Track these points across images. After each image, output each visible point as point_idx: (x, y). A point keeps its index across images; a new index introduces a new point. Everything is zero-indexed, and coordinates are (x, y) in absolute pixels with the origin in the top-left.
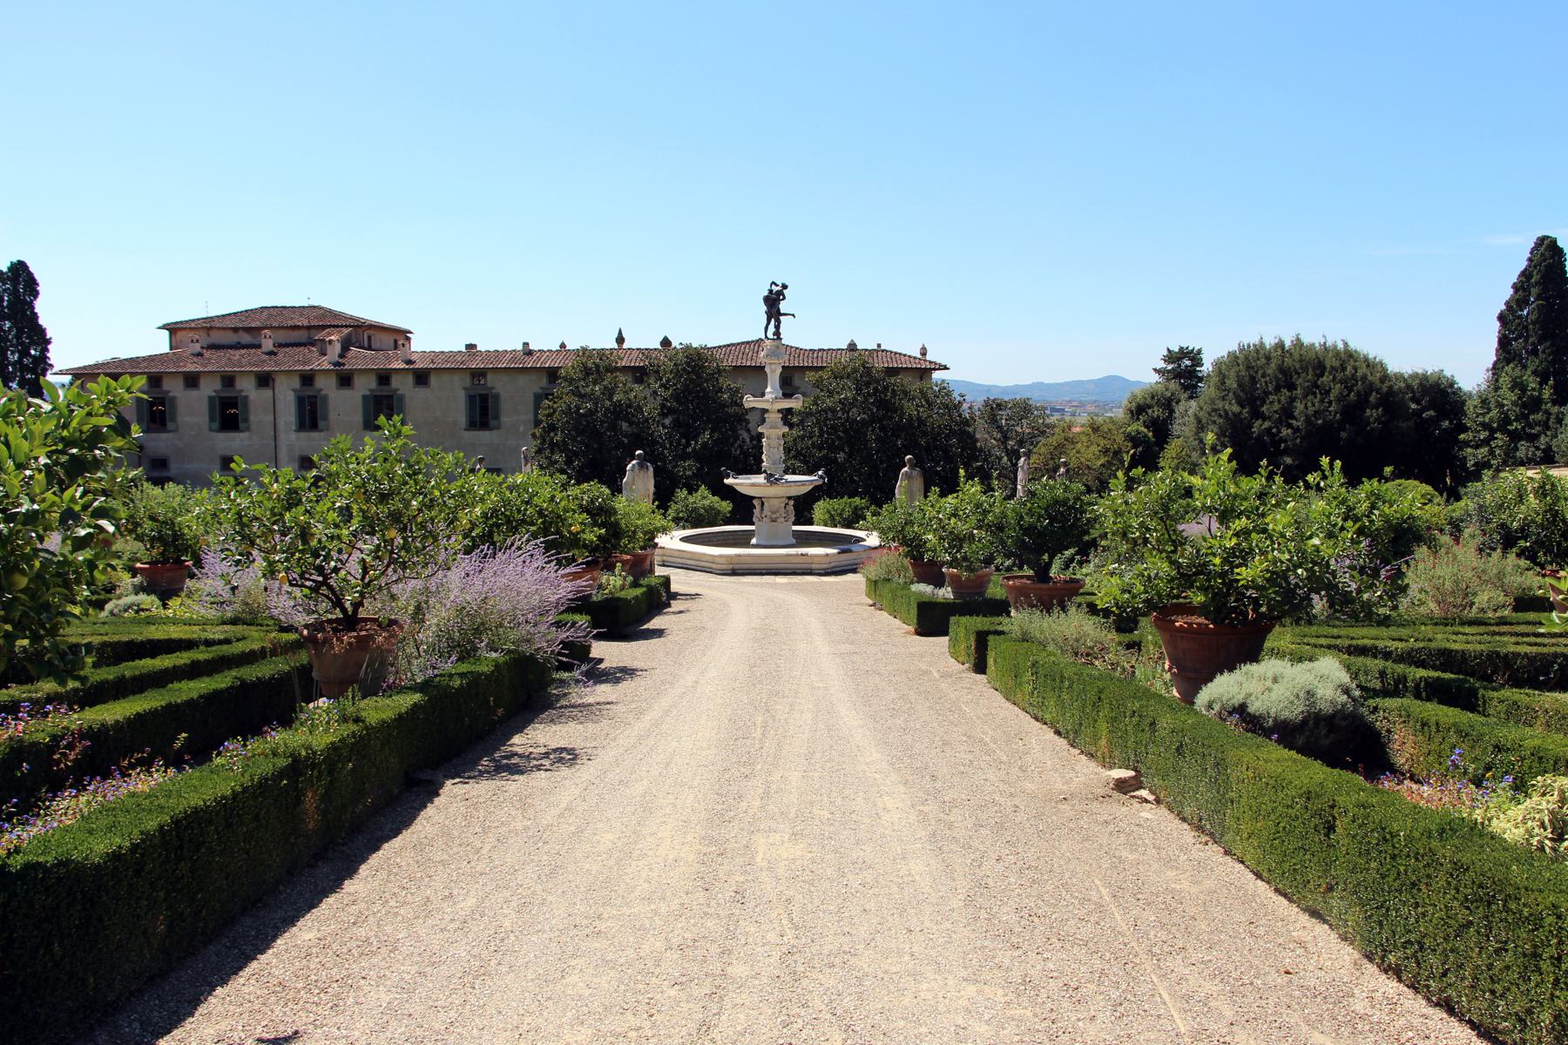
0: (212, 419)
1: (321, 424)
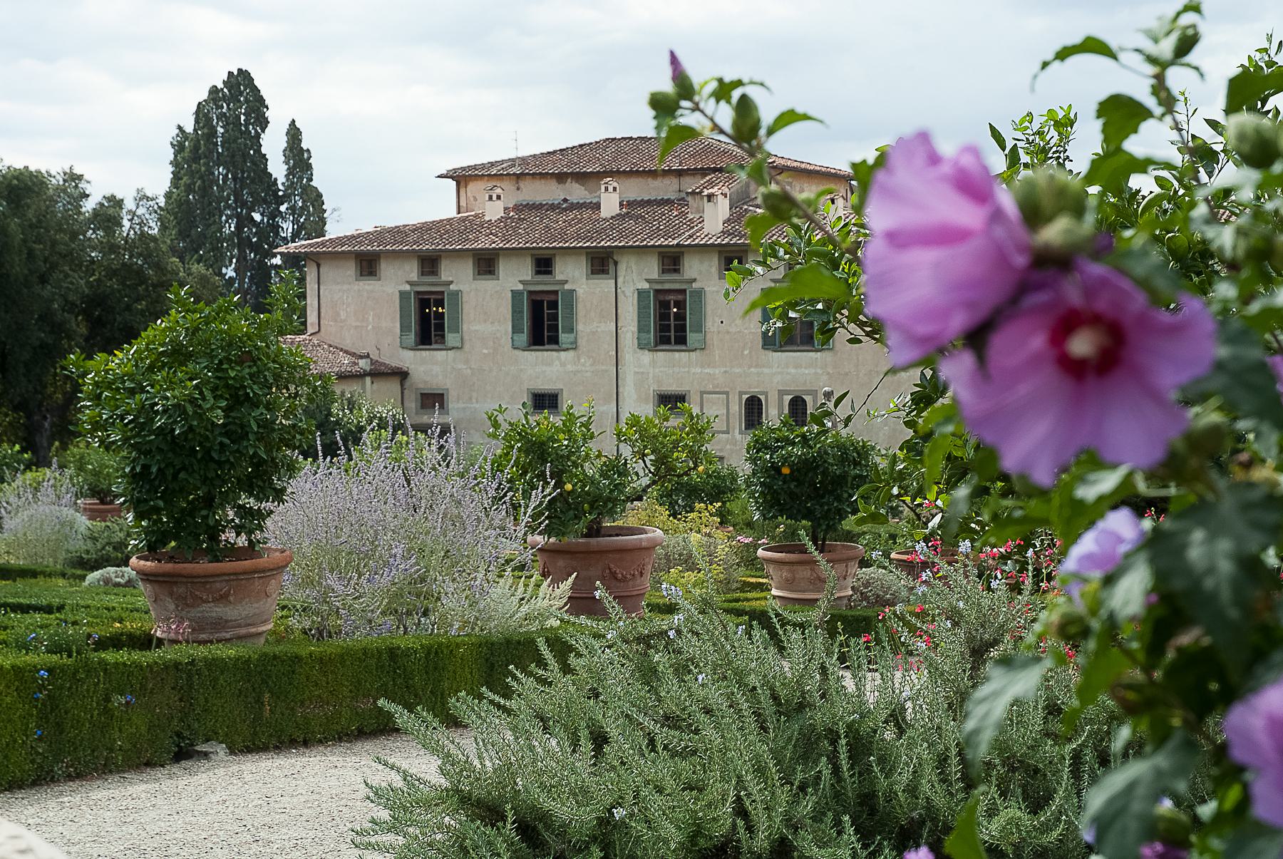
0: (516, 329)
1: (691, 337)
